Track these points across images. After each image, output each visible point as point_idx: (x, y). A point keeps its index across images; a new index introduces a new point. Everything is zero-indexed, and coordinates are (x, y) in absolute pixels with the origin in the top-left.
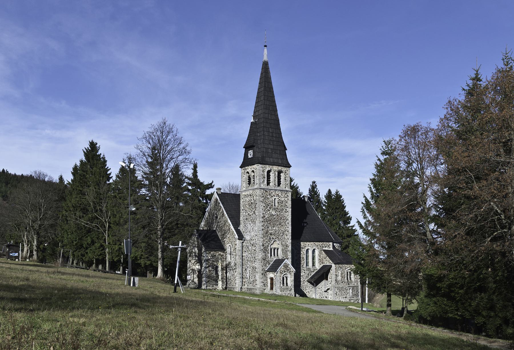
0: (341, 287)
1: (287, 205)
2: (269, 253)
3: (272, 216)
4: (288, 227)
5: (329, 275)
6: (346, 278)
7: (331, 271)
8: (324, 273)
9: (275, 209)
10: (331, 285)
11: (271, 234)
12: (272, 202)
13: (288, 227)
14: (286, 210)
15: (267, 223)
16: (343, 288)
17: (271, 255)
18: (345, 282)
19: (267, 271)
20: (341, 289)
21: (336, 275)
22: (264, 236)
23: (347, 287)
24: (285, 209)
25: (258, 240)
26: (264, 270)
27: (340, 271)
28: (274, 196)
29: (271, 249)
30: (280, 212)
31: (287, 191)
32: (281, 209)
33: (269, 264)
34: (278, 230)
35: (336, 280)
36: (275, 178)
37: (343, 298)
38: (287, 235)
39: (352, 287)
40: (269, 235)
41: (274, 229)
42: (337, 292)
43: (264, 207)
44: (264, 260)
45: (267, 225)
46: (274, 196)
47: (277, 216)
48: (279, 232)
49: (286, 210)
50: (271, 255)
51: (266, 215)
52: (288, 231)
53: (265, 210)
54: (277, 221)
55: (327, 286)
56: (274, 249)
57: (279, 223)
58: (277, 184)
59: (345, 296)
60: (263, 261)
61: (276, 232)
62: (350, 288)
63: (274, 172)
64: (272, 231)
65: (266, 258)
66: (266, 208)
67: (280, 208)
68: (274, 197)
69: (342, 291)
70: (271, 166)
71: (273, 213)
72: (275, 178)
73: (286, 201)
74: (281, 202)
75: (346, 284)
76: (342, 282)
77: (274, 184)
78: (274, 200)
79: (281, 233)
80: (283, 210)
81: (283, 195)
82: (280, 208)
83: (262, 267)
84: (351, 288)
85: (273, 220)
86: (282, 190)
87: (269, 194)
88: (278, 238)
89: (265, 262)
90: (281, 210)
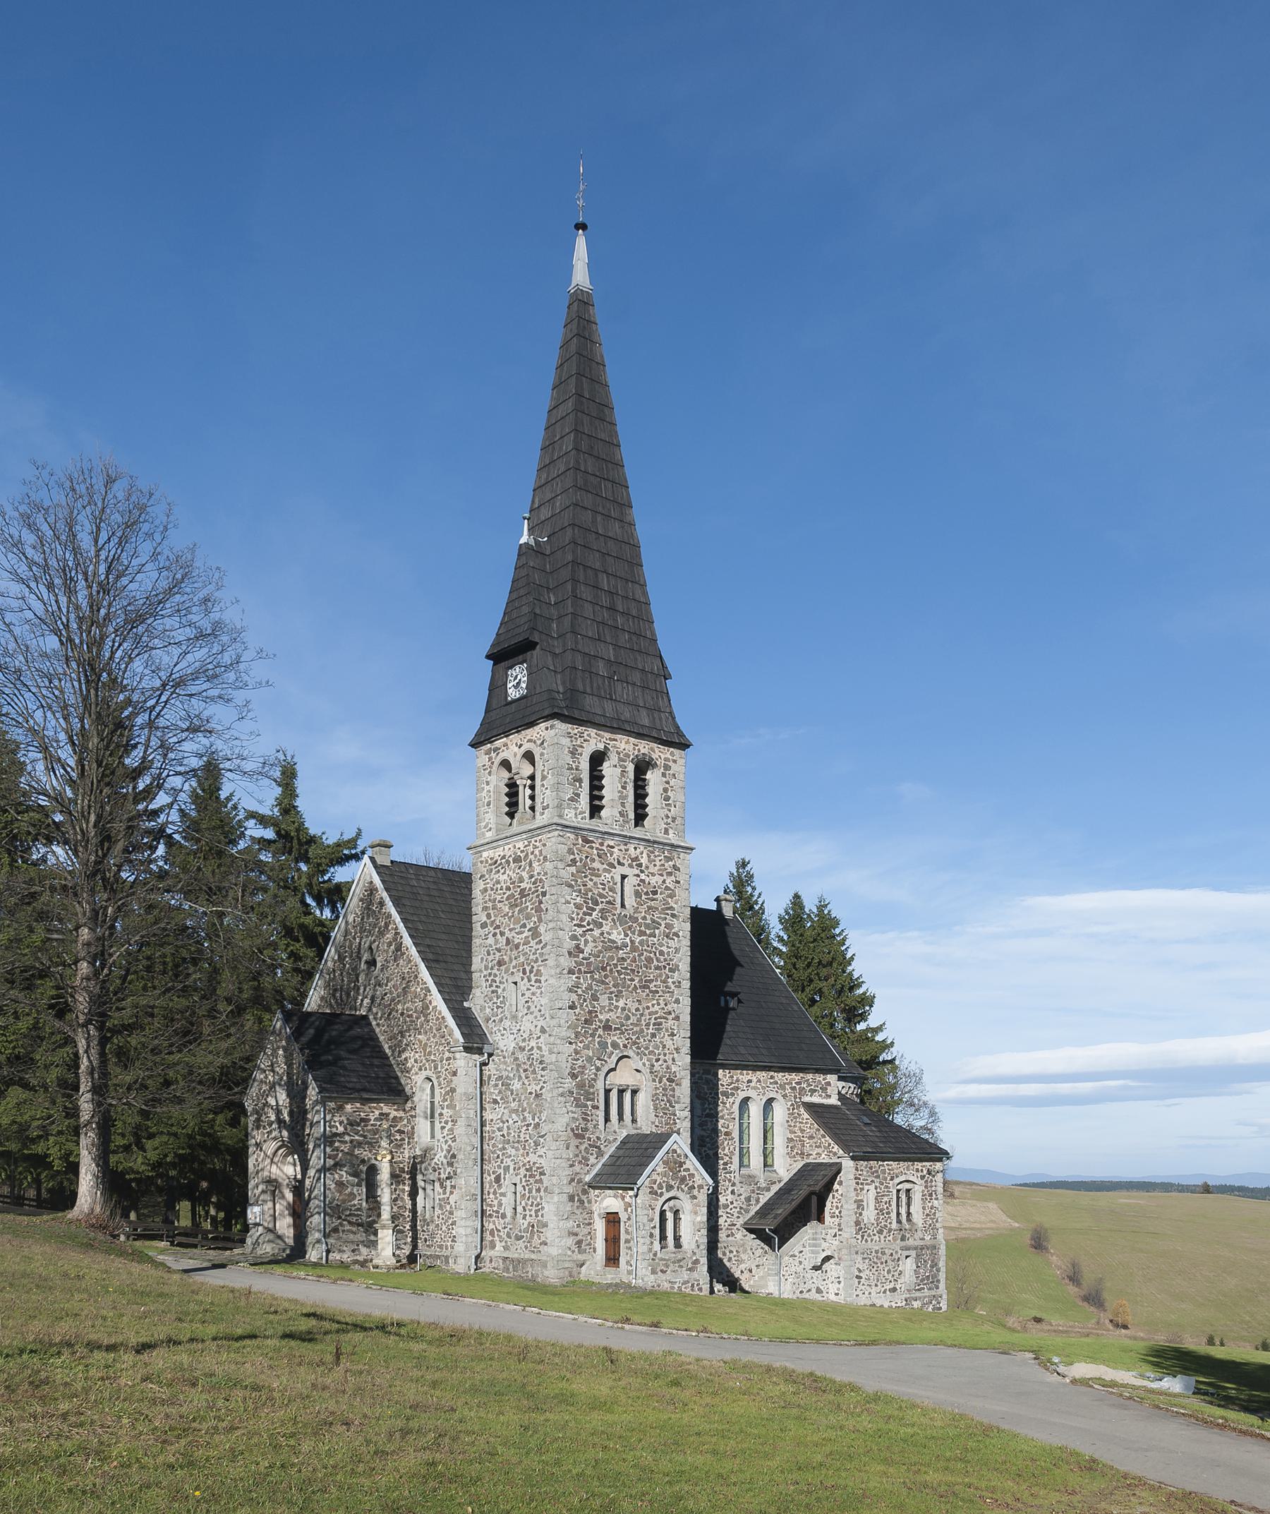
0: (877, 1252)
1: (671, 908)
2: (597, 1108)
3: (610, 949)
4: (677, 1001)
5: (828, 1204)
6: (894, 1215)
7: (836, 1186)
9: (622, 920)
12: (611, 890)
13: (677, 1001)
15: (592, 977)
16: (883, 1253)
17: (607, 1120)
18: (890, 1230)
19: (592, 1186)
20: (875, 1259)
21: (859, 1204)
22: (577, 1034)
23: (898, 1249)
24: (663, 923)
25: (551, 1052)
26: (580, 1181)
27: (872, 1187)
28: (619, 863)
29: (607, 1092)
30: (644, 933)
31: (672, 845)
32: (649, 921)
33: (600, 1154)
34: (637, 1010)
35: (857, 1223)
36: (624, 788)
37: (885, 1292)
38: (673, 1035)
39: (916, 1248)
40: (600, 1031)
41: (621, 1004)
42: (860, 1271)
43: (578, 906)
44: (577, 1136)
45: (590, 987)
46: (619, 863)
47: (634, 949)
50: (607, 1120)
51: (586, 942)
52: (677, 1018)
53: (582, 920)
54: (633, 971)
55: (824, 1245)
56: (621, 1092)
57: (641, 981)
58: (632, 816)
59: (892, 1285)
60: (574, 1142)
61: (628, 1018)
62: (907, 1253)
63: (620, 760)
64: (612, 1016)
65: (586, 1130)
66: (585, 914)
67: (644, 918)
68: (620, 870)
69: (881, 1267)
70: (607, 735)
71: (617, 936)
72: (624, 788)
73: (667, 888)
74: (647, 894)
76: (880, 1232)
77: (621, 814)
78: (618, 879)
79: (648, 1025)
80: (655, 923)
81: (658, 863)
82: (644, 918)
83: (571, 1166)
84: (913, 1253)
85: (616, 965)
86: (655, 842)
88: (635, 1043)
89: (582, 1148)
90: (647, 926)
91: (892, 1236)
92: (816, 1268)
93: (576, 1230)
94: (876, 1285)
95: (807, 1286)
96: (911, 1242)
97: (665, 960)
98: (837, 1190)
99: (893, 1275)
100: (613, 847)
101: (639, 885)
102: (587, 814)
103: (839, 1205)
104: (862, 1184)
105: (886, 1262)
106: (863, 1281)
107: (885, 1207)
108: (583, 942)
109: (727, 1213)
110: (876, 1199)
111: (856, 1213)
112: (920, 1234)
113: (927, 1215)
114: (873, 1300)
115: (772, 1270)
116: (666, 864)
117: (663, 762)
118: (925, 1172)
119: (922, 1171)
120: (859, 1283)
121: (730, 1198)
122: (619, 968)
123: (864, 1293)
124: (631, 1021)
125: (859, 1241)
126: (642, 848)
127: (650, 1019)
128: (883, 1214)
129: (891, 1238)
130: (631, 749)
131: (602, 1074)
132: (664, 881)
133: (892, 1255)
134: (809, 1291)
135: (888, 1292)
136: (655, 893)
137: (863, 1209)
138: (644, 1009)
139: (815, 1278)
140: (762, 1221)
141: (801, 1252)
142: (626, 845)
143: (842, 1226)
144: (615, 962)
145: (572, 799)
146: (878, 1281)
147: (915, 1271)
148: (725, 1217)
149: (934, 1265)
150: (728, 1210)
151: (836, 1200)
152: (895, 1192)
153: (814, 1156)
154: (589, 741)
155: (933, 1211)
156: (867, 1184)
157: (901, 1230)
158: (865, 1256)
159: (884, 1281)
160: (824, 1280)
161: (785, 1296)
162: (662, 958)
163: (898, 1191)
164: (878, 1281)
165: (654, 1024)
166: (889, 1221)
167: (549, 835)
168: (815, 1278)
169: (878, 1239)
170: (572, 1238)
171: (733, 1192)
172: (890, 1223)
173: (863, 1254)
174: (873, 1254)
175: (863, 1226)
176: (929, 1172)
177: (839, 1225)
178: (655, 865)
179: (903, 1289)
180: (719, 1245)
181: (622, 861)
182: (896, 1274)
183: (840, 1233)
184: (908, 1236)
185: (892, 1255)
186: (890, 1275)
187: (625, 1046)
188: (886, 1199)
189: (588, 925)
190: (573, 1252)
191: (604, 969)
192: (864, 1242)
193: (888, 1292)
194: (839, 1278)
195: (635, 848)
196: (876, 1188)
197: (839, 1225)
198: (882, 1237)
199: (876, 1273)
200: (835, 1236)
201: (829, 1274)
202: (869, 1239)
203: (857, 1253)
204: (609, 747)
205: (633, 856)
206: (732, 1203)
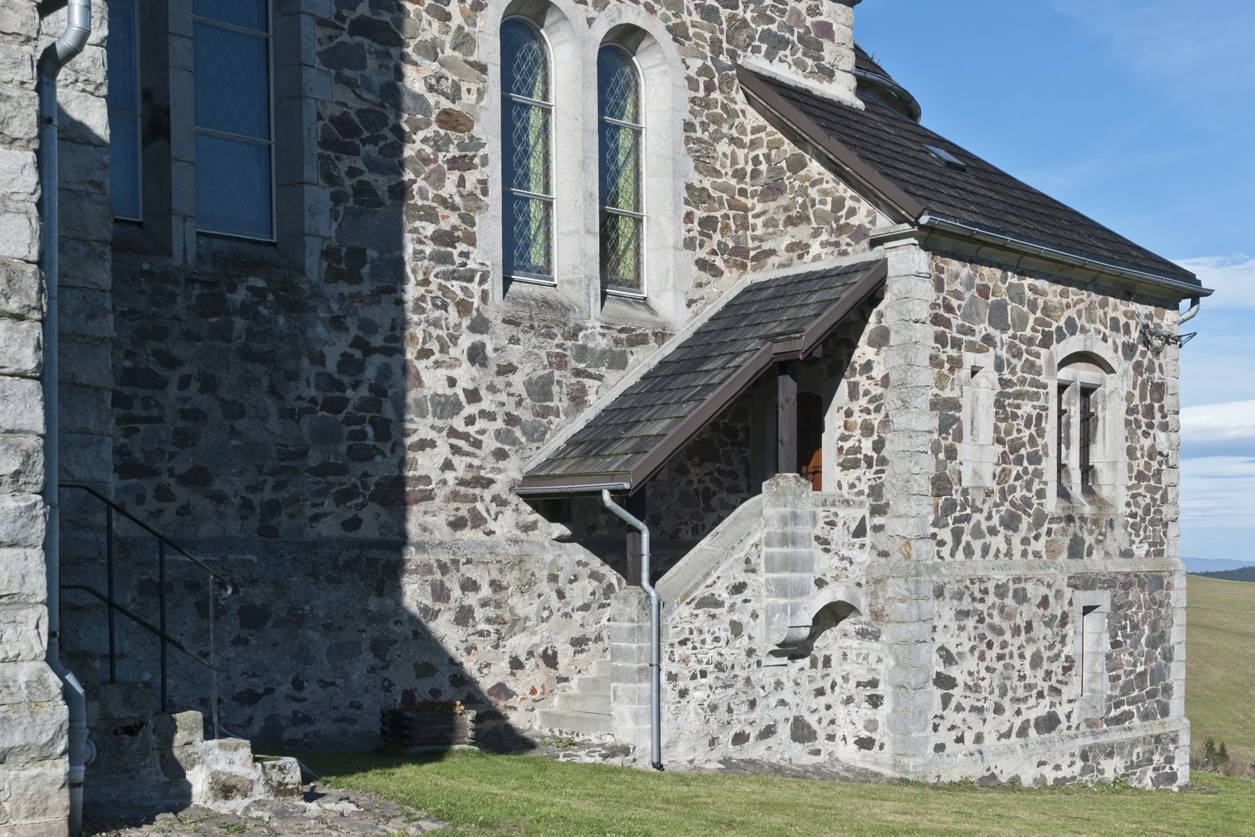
0: (1001, 591)
6: (1049, 467)
7: (863, 352)
8: (782, 366)
10: (863, 557)
16: (1021, 597)
18: (1040, 519)
23: (1062, 582)
27: (986, 360)
35: (941, 484)
37: (1023, 732)
42: (948, 658)
55: (825, 564)
59: (1042, 709)
62: (1084, 598)
69: (1014, 643)
75: (1052, 551)
76: (1011, 522)
84: (1103, 598)
91: (1044, 539)
92: (793, 649)
94: (999, 710)
95: (762, 716)
96: (1096, 563)
98: (868, 366)
99: (1048, 674)
103: (876, 419)
104: (956, 344)
105: (1029, 627)
106: (957, 692)
107: (1026, 434)
109: (453, 433)
110: (999, 404)
111: (936, 449)
112: (1118, 538)
113: (1141, 476)
114: (991, 761)
115: (626, 655)
118: (1135, 335)
119: (1127, 330)
120: (946, 700)
121: (466, 374)
123: (960, 740)
125: (946, 551)
128: (1019, 461)
129: (1040, 546)
133: (1044, 603)
134: (768, 732)
135: (1032, 732)
137: (959, 437)
139: (789, 685)
140: (591, 466)
141: (738, 588)
143: (888, 495)
146: (1003, 694)
147: (1108, 657)
148: (442, 451)
149: (1158, 639)
150: (458, 423)
151: (863, 401)
152: (1053, 389)
153: (783, 256)
155: (1155, 465)
156: (972, 347)
157: (1070, 519)
158: (966, 604)
159: (1021, 693)
160: (820, 692)
161: (678, 757)
163: (1062, 388)
164: (1003, 694)
166: (1036, 486)
168: (789, 685)
169: (1003, 548)
171: (476, 355)
172: (1041, 494)
173: (959, 596)
174: (991, 598)
175: (958, 497)
176: (1146, 336)
177: (876, 491)
179: (1075, 720)
180: (412, 556)
182: (1057, 667)
183: (878, 520)
184: (1089, 540)
185: (1044, 603)
186: (1040, 673)
188: (1027, 408)
192: (960, 555)
193: (1032, 732)
194: (874, 683)
196: (999, 366)
197: (876, 491)
198: (1016, 540)
199: (999, 666)
200: (860, 531)
201: (836, 671)
202: (977, 546)
203: (939, 593)
206: (473, 396)
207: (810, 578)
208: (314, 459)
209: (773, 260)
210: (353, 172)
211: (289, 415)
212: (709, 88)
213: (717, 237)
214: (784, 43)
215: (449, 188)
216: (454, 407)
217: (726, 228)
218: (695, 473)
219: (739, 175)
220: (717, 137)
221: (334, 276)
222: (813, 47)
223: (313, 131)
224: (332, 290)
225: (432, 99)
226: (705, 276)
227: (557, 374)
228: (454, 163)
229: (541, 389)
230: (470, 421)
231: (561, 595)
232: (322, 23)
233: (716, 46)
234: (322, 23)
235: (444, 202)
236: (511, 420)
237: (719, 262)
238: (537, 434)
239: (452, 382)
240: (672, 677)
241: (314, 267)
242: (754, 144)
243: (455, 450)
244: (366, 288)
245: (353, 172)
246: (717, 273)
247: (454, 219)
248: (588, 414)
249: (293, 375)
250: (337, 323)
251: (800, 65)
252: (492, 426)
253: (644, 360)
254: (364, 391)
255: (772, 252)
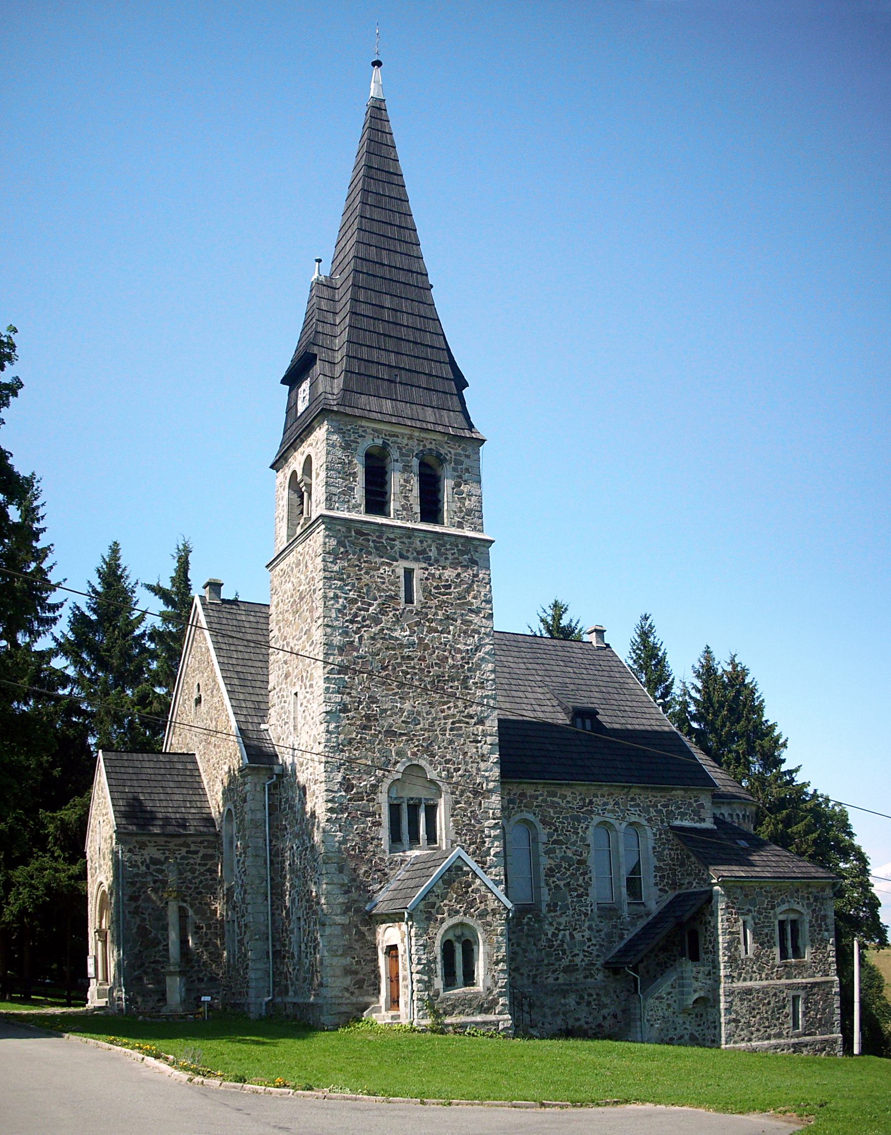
11: (390, 733)
14: (464, 622)
29: (394, 809)
36: (407, 481)
41: (407, 706)
48: (432, 725)
49: (464, 622)
53: (356, 615)
58: (417, 509)
63: (402, 455)
66: (360, 609)
74: (437, 588)
81: (450, 557)
82: (436, 614)
85: (400, 665)
87: (377, 548)
93: (355, 967)
95: (680, 1032)
97: (463, 658)
100: (394, 540)
101: (427, 579)
102: (363, 508)
108: (357, 640)
116: (461, 558)
117: (453, 457)
122: (404, 668)
124: (421, 726)
126: (430, 542)
127: (445, 723)
130: (415, 444)
131: (384, 787)
132: (458, 575)
136: (449, 587)
138: (437, 713)
139: (688, 1023)
142: (410, 538)
144: (399, 661)
145: (343, 493)
154: (364, 437)
162: (459, 656)
165: (452, 730)
167: (318, 530)
170: (349, 978)
178: (446, 559)
181: (405, 553)
187: (414, 754)
189: (364, 620)
190: (352, 993)
191: (384, 668)
195: (421, 542)
204: (389, 443)
205: (419, 549)
207: (692, 990)
208: (546, 962)
209: (684, 886)
210: (554, 882)
211: (540, 950)
212: (660, 835)
213: (666, 880)
214: (687, 814)
215: (581, 881)
216: (584, 943)
217: (669, 877)
218: (661, 956)
219: (672, 860)
220: (664, 850)
221: (549, 911)
222: (696, 813)
223: (543, 873)
224: (549, 915)
225: (574, 857)
226: (661, 894)
227: (614, 931)
228: (581, 874)
229: (610, 935)
230: (589, 947)
231: (618, 997)
232: (544, 843)
233: (662, 821)
234: (544, 843)
235: (578, 885)
236: (601, 945)
237: (667, 888)
238: (609, 949)
239: (583, 936)
240: (648, 1021)
241: (544, 909)
242: (677, 849)
243: (585, 956)
244: (558, 913)
245: (554, 882)
246: (667, 892)
247: (582, 890)
248: (625, 941)
249: (539, 940)
250: (551, 924)
251: (693, 819)
252: (595, 948)
253: (641, 923)
254: (559, 942)
255: (683, 884)
